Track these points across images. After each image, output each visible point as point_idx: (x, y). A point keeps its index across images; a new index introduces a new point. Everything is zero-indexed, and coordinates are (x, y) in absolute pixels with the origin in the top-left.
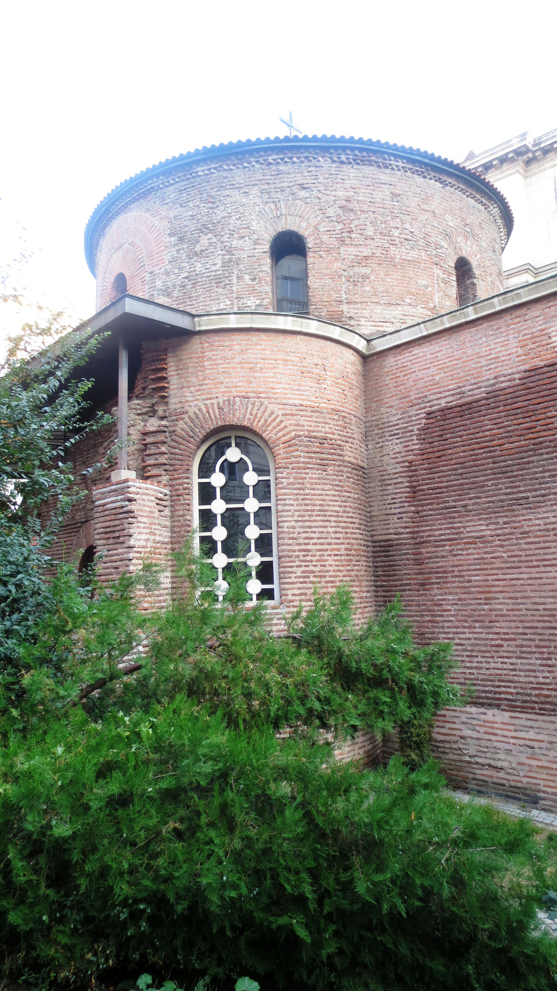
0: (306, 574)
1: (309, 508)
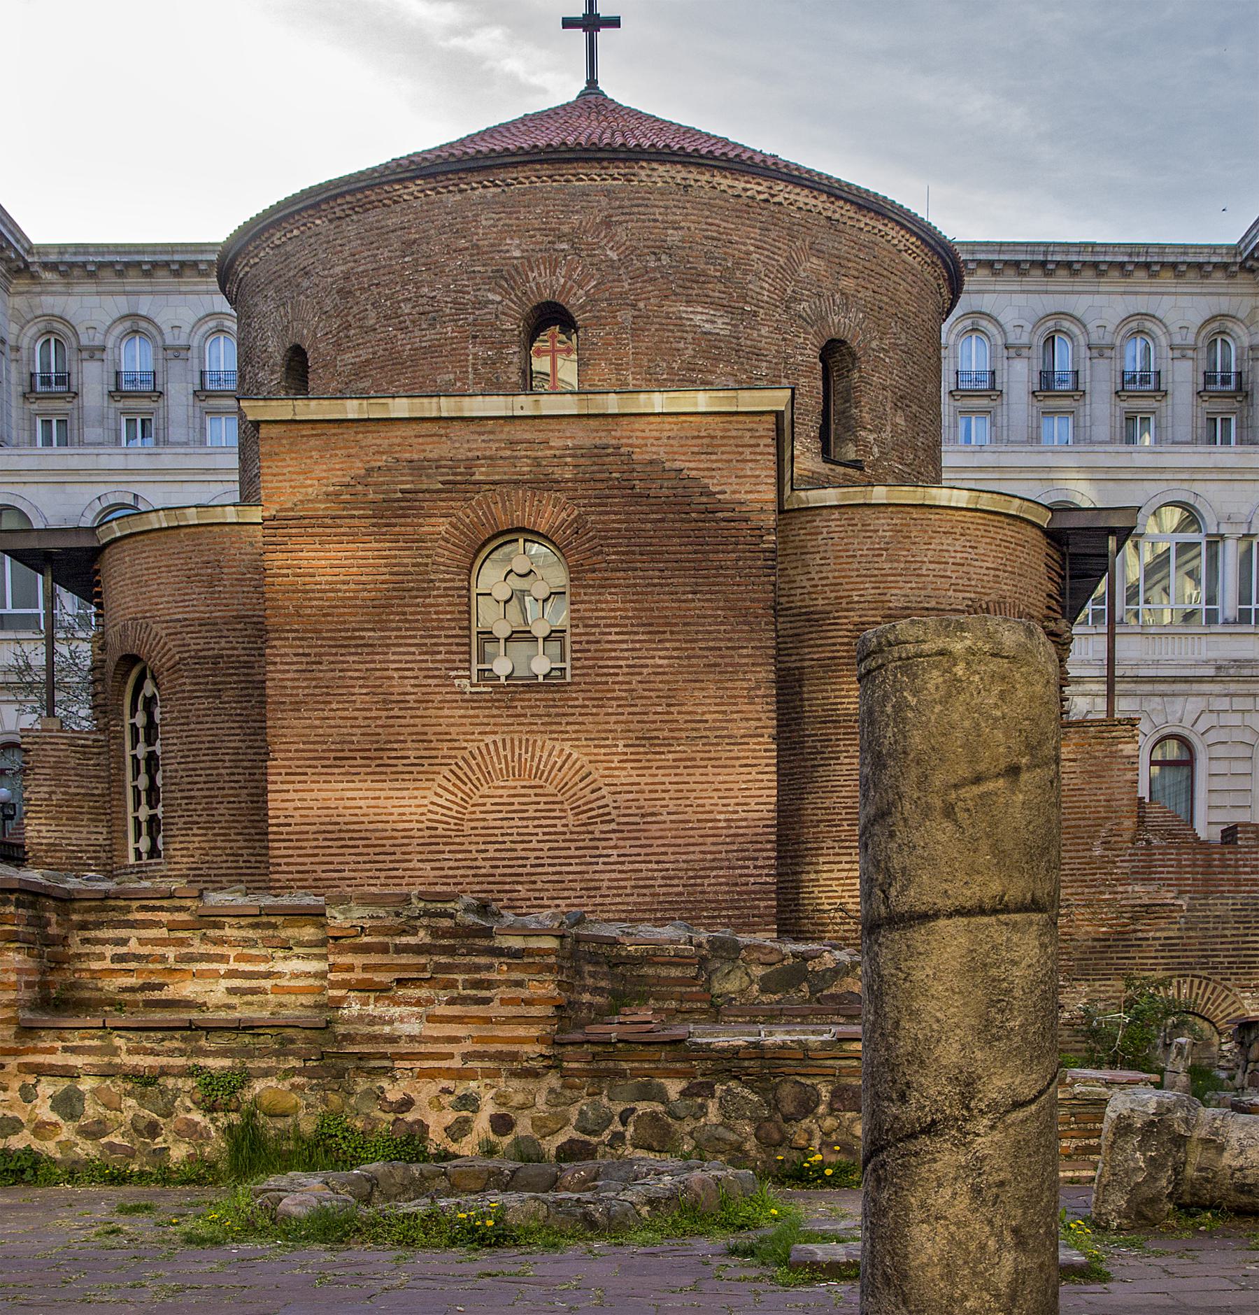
1: (194, 746)
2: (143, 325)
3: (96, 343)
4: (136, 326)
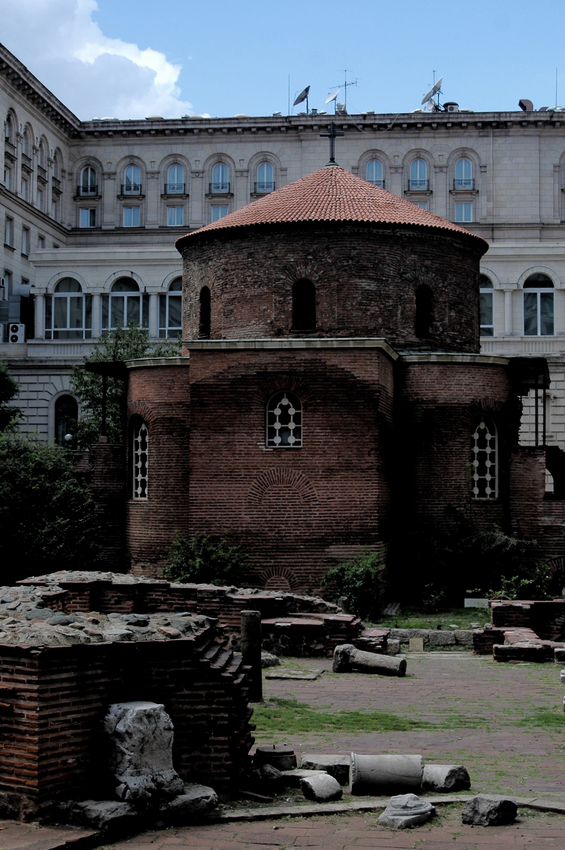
0: (158, 486)
2: (136, 160)
3: (112, 170)
4: (132, 161)
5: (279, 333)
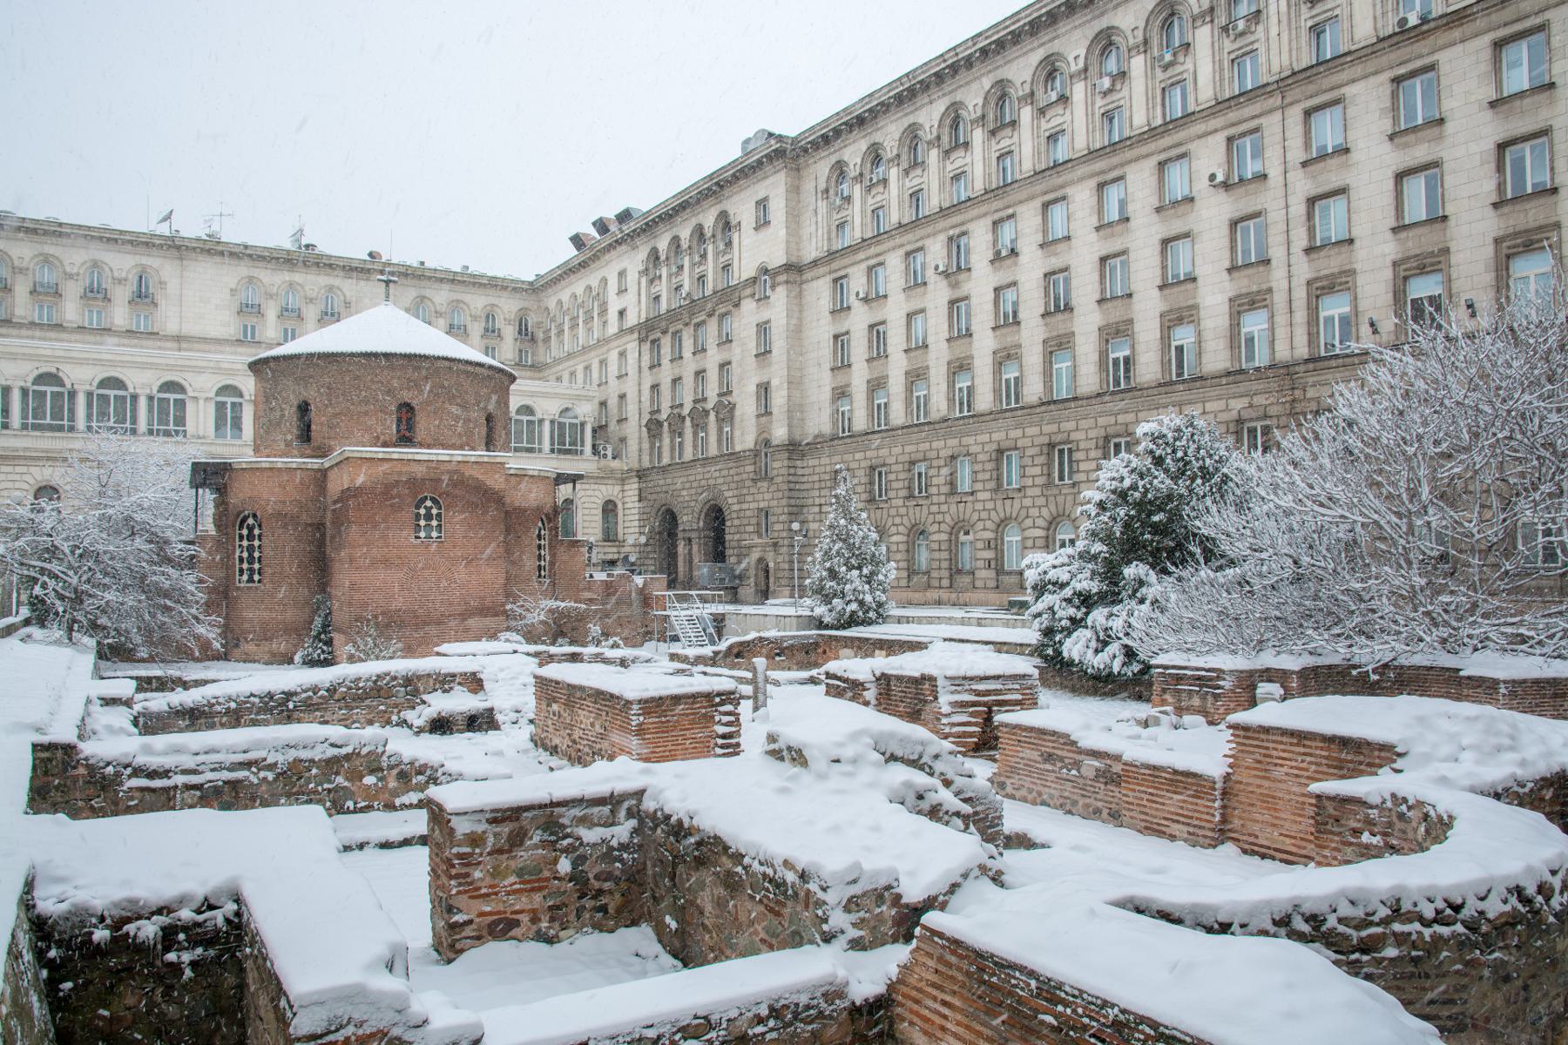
5: (385, 445)
